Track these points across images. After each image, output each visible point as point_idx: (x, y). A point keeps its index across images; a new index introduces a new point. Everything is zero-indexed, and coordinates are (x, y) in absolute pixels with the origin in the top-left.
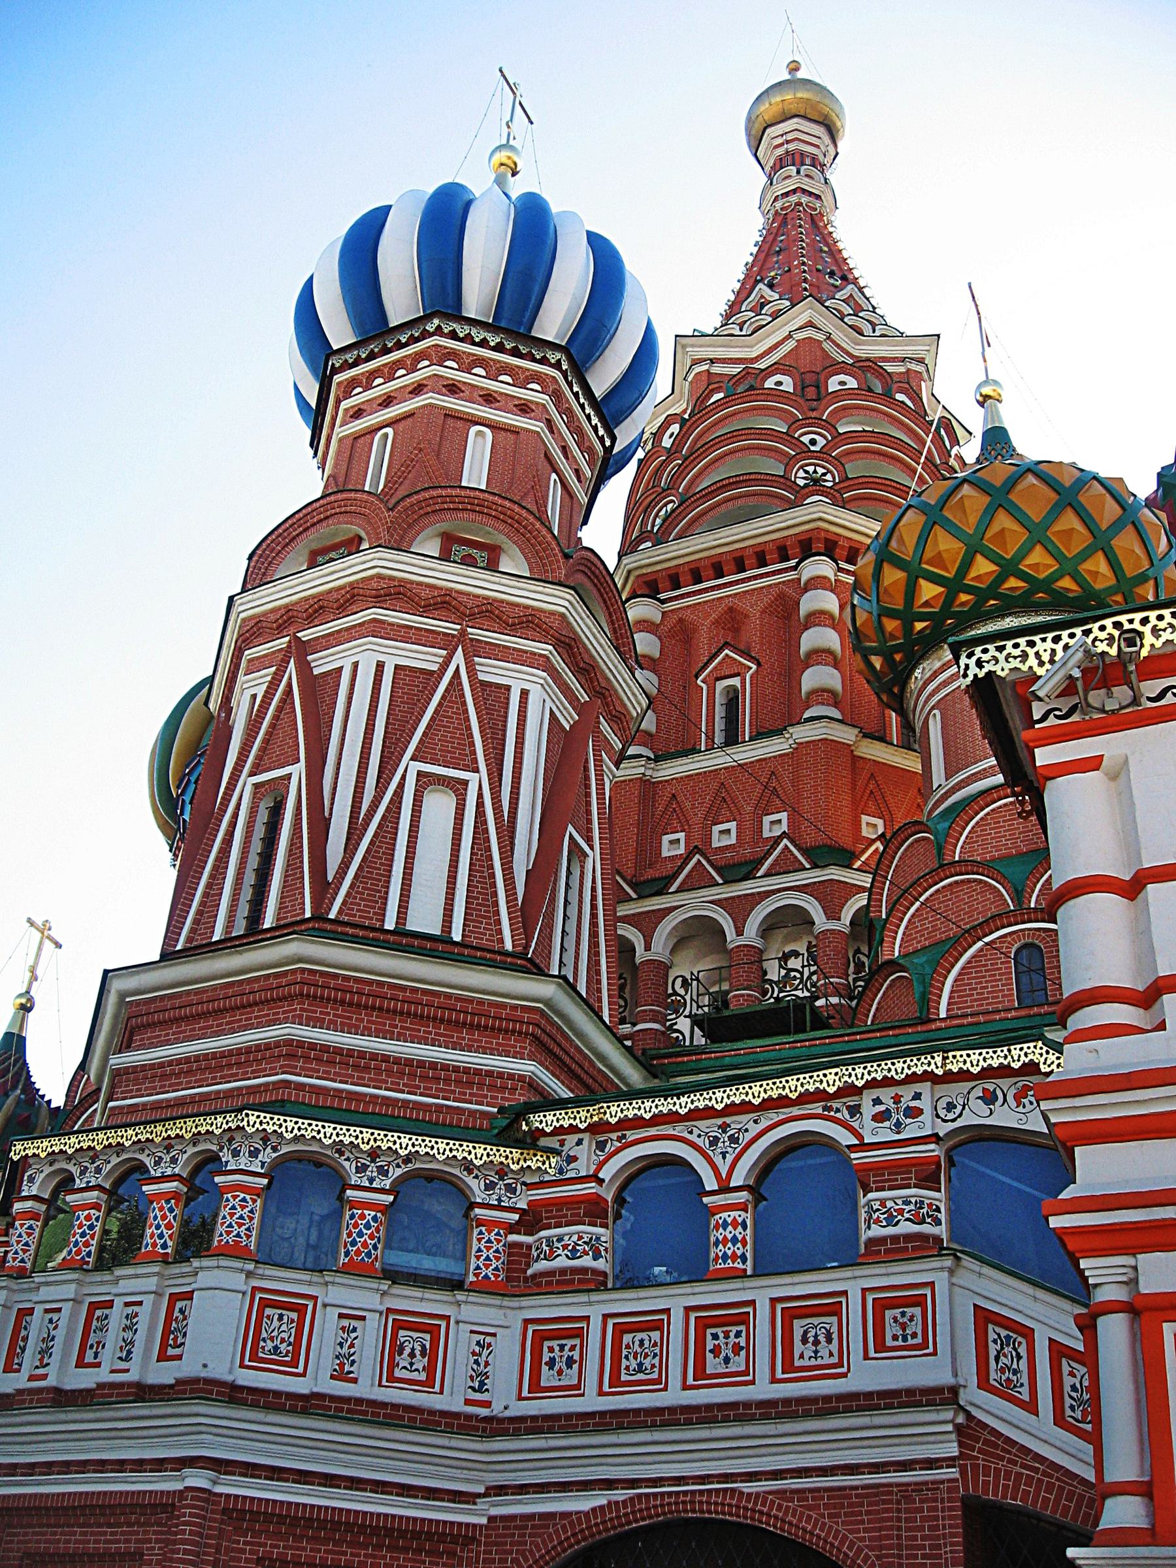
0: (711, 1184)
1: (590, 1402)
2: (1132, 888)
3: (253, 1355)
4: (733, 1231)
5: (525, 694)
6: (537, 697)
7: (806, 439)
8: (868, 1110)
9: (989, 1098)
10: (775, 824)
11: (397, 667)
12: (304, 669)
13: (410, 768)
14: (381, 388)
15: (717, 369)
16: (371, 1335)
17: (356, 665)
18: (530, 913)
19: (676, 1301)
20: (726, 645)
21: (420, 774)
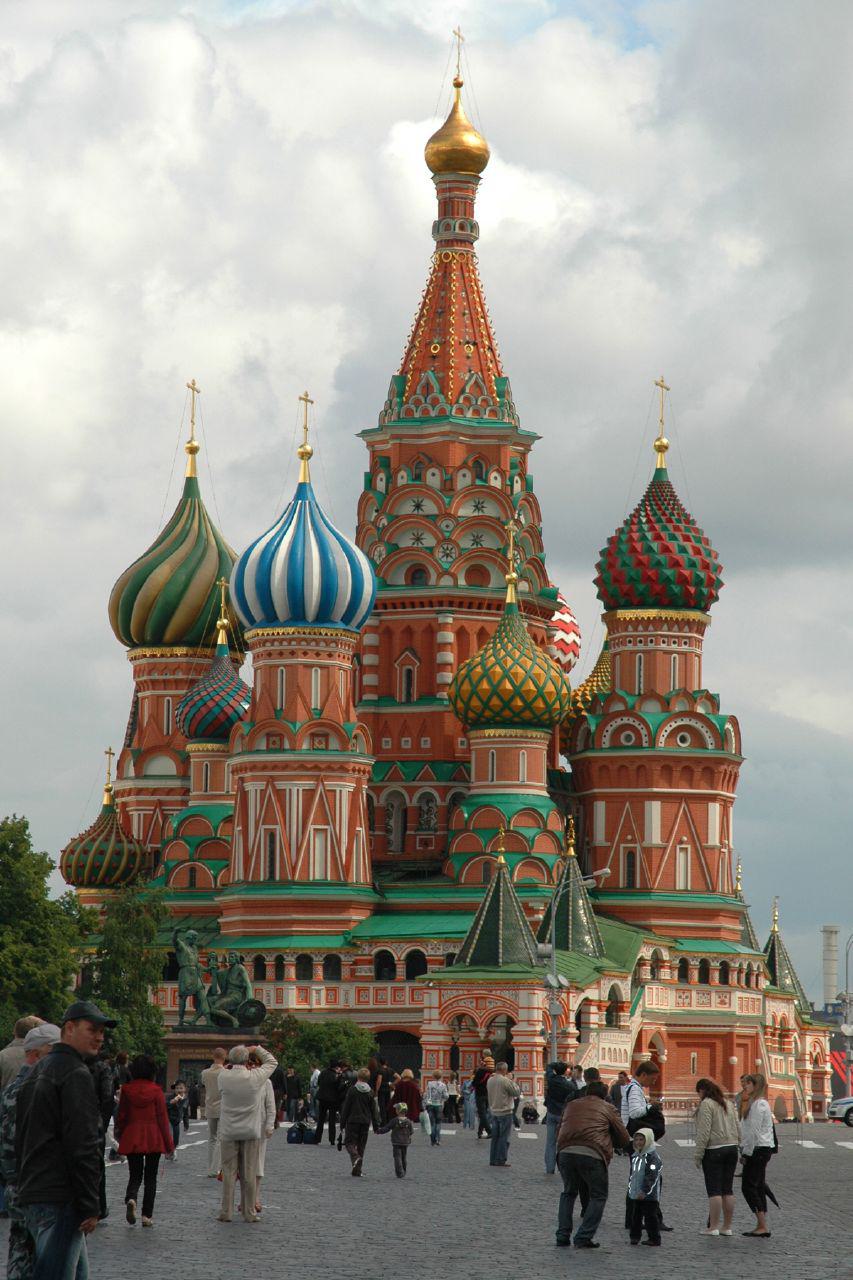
0: (396, 958)
1: (371, 1006)
2: (430, 1008)
3: (298, 1003)
4: (401, 971)
5: (341, 791)
6: (345, 788)
7: (443, 526)
8: (430, 947)
9: (454, 947)
10: (426, 743)
11: (303, 790)
12: (274, 787)
13: (311, 827)
14: (277, 647)
15: (405, 441)
16: (323, 993)
17: (290, 790)
18: (347, 868)
19: (389, 985)
20: (406, 649)
21: (315, 829)
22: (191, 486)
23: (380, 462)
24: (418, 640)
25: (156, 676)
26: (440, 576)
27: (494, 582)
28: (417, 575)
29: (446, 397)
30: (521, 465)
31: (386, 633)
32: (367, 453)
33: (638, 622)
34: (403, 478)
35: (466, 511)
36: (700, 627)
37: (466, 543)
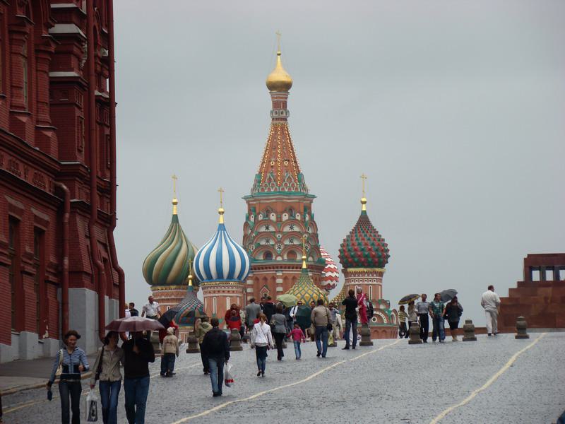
15: (262, 201)
22: (175, 218)
23: (252, 210)
24: (269, 281)
25: (163, 297)
26: (277, 257)
27: (299, 258)
28: (268, 255)
29: (277, 184)
30: (307, 209)
31: (257, 279)
32: (246, 206)
33: (355, 273)
34: (261, 218)
35: (287, 229)
36: (381, 274)
37: (287, 242)
